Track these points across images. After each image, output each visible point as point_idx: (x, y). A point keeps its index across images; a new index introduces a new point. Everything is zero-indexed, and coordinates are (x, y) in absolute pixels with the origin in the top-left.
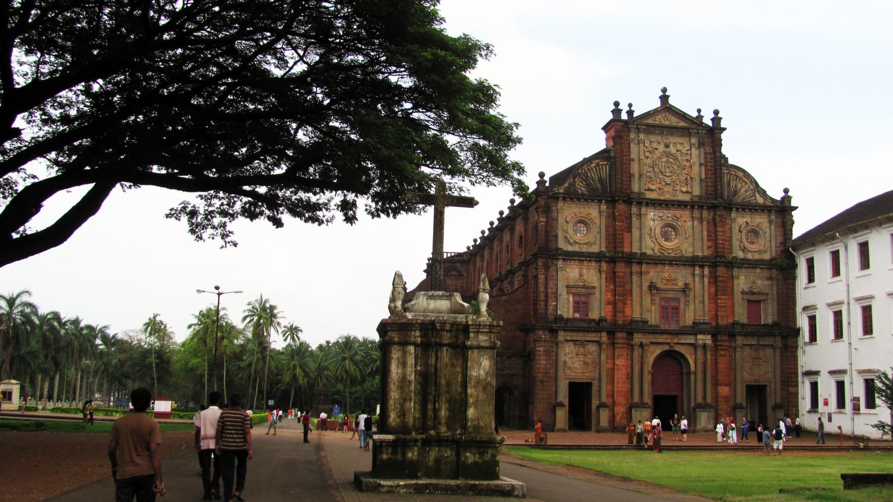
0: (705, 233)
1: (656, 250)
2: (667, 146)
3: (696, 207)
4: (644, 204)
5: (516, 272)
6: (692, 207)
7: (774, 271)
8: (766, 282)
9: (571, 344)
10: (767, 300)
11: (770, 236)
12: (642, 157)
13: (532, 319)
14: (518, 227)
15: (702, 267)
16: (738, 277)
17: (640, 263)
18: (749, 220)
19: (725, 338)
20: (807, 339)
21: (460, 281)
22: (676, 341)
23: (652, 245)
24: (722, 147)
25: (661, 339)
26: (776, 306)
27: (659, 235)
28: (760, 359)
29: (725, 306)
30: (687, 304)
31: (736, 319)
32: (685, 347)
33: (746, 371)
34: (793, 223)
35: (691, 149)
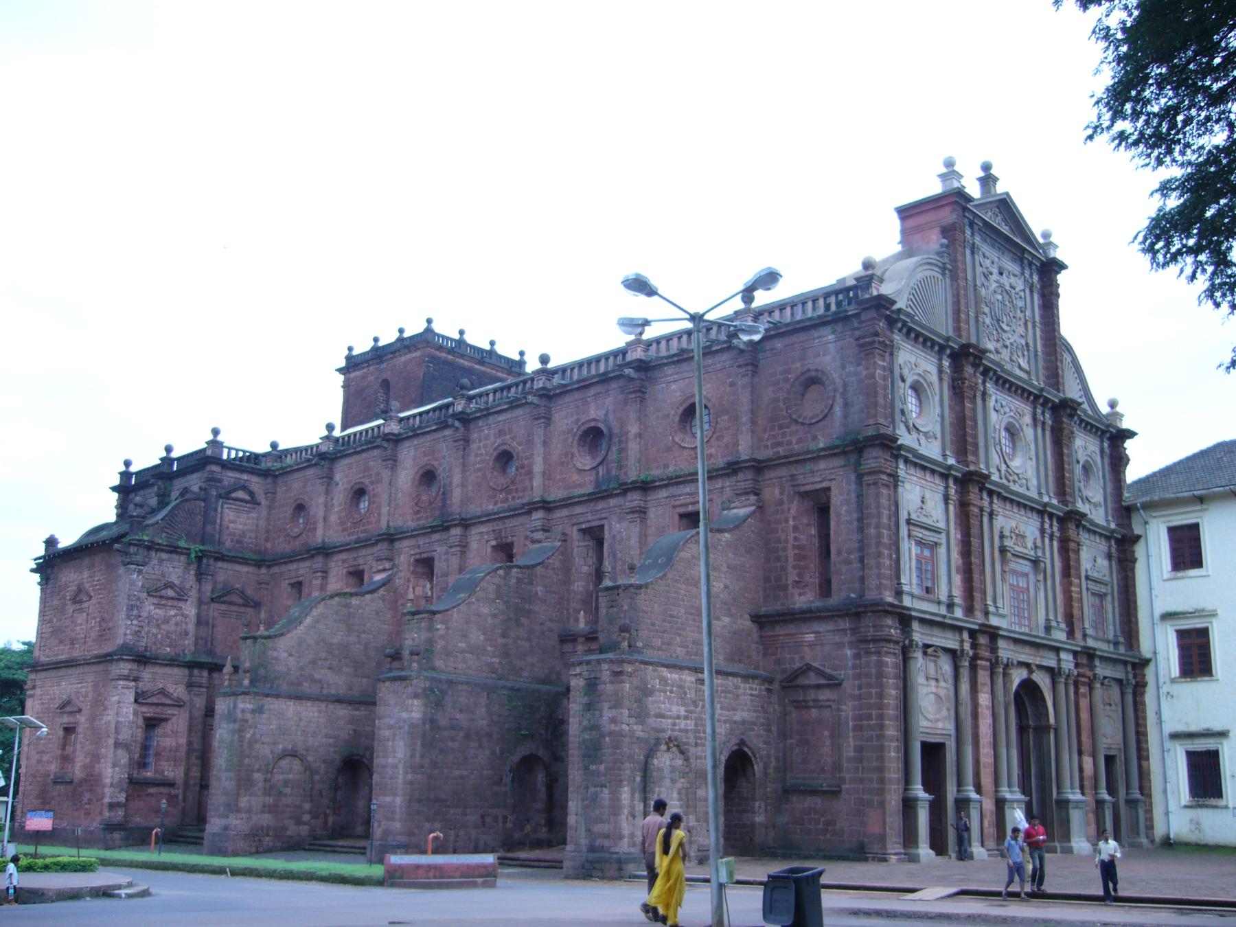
0: (1049, 452)
1: (1003, 472)
3: (1041, 401)
5: (666, 486)
7: (1113, 542)
9: (918, 655)
11: (1104, 476)
12: (978, 283)
13: (796, 591)
14: (673, 387)
15: (1051, 516)
20: (1175, 671)
21: (254, 515)
24: (1060, 300)
28: (1110, 705)
30: (1037, 589)
34: (1128, 460)
35: (1024, 291)
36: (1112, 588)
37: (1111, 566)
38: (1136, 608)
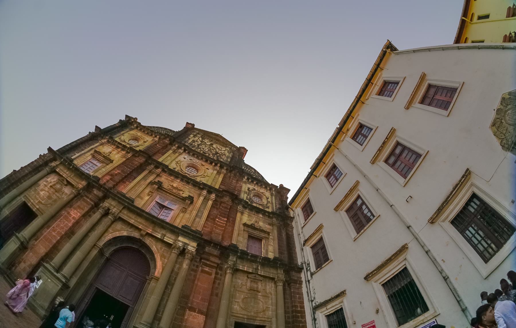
0: (220, 179)
2: (212, 144)
3: (219, 165)
4: (183, 148)
6: (216, 165)
7: (274, 219)
8: (268, 226)
10: (268, 238)
15: (210, 192)
16: (242, 213)
17: (157, 167)
18: (256, 189)
19: (216, 252)
20: (313, 268)
22: (150, 231)
23: (175, 166)
25: (133, 219)
26: (277, 246)
27: (184, 167)
29: (223, 226)
31: (234, 242)
32: (159, 245)
33: (238, 302)
34: (288, 198)
36: (273, 237)
37: (273, 228)
38: (294, 247)
